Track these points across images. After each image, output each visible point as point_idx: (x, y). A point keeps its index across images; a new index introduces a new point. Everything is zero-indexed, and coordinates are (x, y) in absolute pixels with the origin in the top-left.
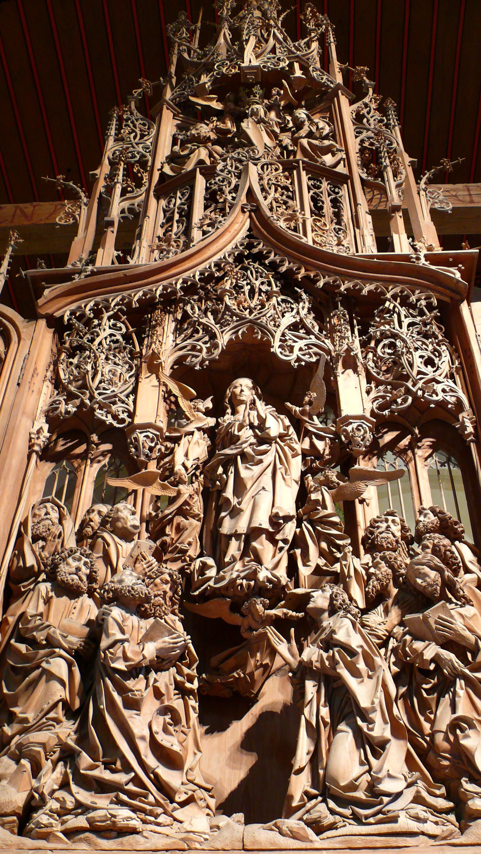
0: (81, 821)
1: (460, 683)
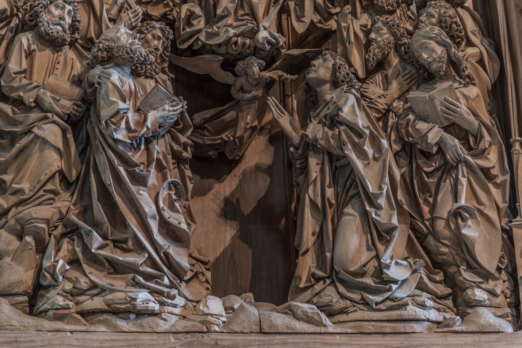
0: (98, 303)
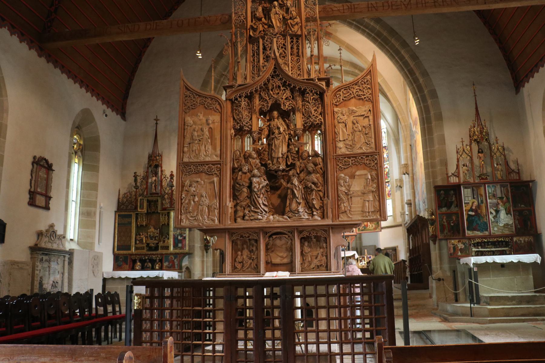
1: (314, 191)
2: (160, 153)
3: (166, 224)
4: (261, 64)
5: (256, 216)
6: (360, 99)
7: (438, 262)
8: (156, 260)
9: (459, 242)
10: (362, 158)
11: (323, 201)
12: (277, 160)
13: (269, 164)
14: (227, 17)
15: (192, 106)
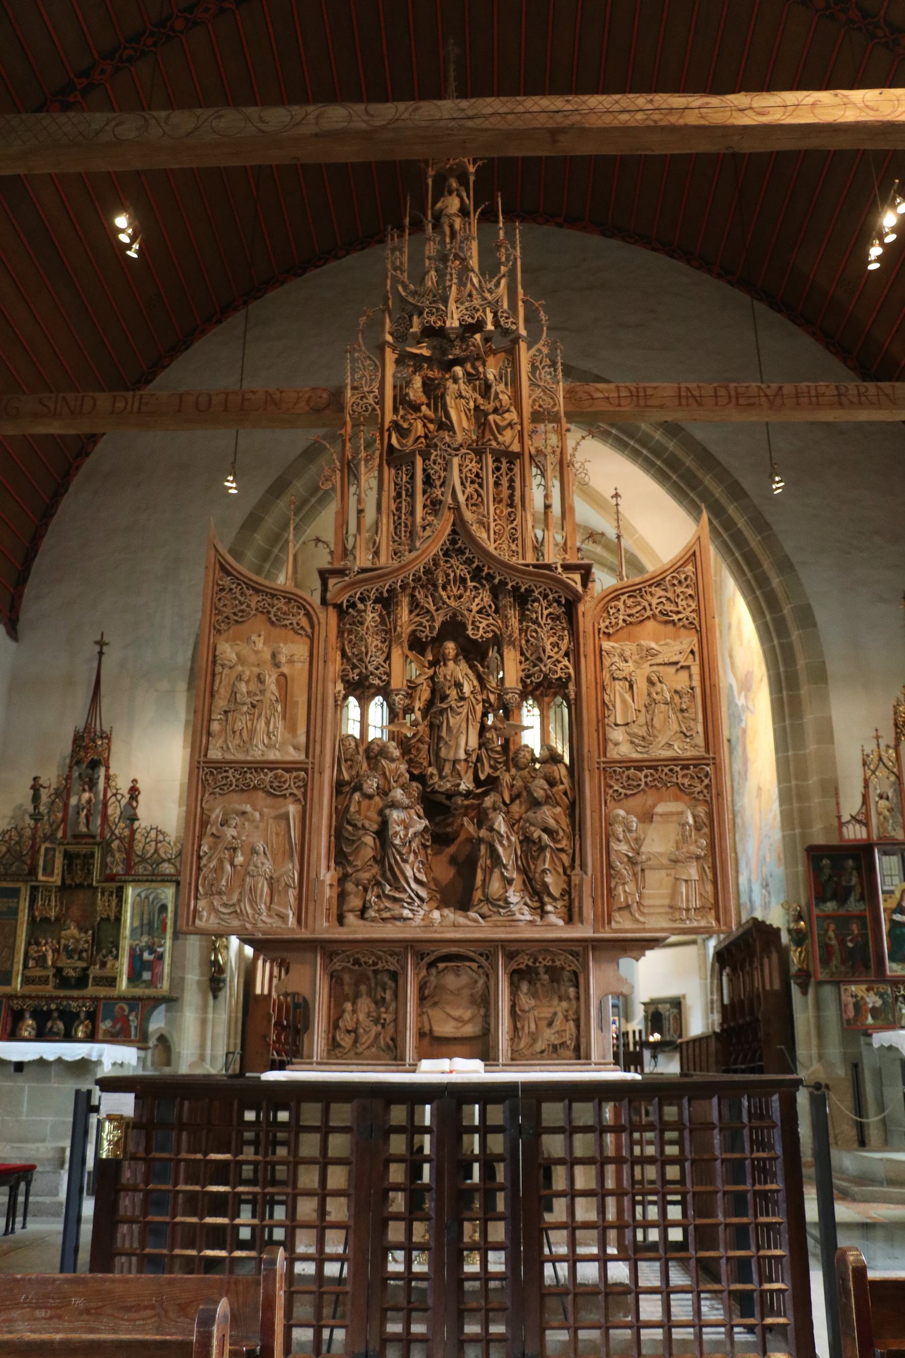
0: (386, 915)
1: (548, 850)
2: (104, 729)
3: (112, 918)
4: (419, 519)
5: (397, 910)
6: (667, 622)
7: (814, 1042)
8: (77, 1015)
9: (868, 990)
10: (671, 770)
11: (569, 876)
12: (454, 766)
13: (432, 775)
14: (325, 395)
15: (235, 614)
